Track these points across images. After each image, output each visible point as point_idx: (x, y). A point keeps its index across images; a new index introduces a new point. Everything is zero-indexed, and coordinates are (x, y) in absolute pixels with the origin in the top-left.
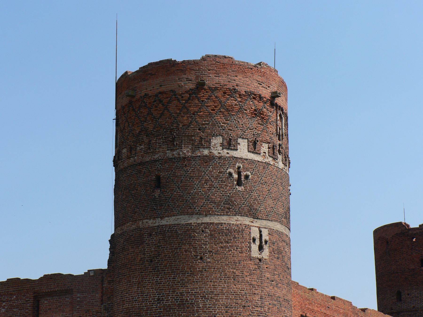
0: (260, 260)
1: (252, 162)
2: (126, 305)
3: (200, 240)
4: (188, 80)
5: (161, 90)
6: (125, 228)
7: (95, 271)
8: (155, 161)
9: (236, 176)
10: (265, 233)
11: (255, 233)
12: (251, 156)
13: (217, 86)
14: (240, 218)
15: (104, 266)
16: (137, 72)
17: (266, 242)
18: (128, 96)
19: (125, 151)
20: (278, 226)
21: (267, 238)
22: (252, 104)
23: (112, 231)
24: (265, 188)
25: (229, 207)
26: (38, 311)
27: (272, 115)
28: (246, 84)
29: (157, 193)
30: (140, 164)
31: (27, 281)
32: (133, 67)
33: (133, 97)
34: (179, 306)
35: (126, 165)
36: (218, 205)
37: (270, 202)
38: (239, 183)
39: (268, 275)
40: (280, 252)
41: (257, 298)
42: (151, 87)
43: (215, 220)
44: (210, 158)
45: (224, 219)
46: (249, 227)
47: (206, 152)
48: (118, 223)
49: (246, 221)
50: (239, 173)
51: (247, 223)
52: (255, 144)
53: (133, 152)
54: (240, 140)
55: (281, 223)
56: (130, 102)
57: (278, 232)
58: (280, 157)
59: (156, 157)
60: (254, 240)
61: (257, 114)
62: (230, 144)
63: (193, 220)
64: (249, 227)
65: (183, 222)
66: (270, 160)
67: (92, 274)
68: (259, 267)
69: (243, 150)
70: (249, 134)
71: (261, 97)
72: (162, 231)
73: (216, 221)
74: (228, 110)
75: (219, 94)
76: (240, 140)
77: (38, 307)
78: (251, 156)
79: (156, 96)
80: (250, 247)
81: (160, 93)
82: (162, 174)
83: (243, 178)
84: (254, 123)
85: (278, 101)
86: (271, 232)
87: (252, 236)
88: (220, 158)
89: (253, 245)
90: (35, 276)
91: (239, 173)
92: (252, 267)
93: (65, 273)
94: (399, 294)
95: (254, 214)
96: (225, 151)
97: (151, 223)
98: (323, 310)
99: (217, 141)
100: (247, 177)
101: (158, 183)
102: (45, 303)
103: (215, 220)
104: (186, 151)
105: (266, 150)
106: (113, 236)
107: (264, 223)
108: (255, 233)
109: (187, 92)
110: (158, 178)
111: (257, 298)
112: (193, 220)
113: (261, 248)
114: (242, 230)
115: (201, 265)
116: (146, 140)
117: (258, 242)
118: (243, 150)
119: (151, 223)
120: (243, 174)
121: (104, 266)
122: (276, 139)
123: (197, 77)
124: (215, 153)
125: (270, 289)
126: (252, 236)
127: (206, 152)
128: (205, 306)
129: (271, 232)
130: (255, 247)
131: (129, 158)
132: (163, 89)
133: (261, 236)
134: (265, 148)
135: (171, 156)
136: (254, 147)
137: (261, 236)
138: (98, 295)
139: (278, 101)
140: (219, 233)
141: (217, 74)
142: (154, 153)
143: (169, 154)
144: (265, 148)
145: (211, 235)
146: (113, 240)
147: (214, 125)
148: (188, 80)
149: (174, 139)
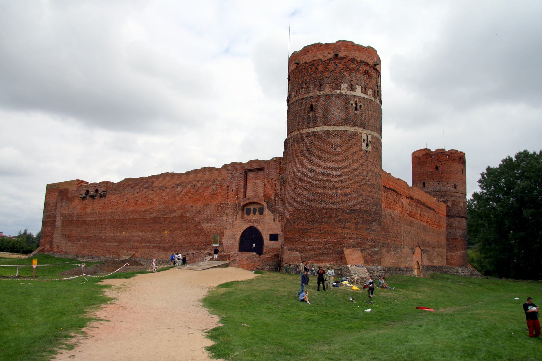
0: (367, 152)
1: (363, 98)
2: (293, 174)
3: (334, 139)
4: (328, 53)
5: (314, 59)
6: (293, 134)
7: (276, 158)
8: (310, 97)
9: (354, 105)
10: (370, 137)
11: (364, 137)
12: (363, 95)
13: (345, 56)
14: (356, 128)
15: (282, 156)
16: (301, 51)
17: (370, 142)
18: (296, 63)
19: (293, 93)
20: (376, 134)
21: (371, 140)
22: (363, 68)
23: (285, 137)
26: (246, 179)
27: (375, 75)
29: (311, 114)
30: (301, 99)
31: (241, 164)
32: (299, 49)
33: (298, 64)
34: (322, 175)
35: (294, 100)
36: (345, 120)
37: (373, 121)
38: (356, 109)
39: (371, 160)
40: (377, 149)
41: (365, 172)
42: (308, 58)
46: (361, 133)
47: (338, 92)
48: (289, 133)
49: (360, 130)
50: (356, 104)
51: (360, 131)
52: (365, 88)
53: (298, 93)
54: (357, 86)
55: (378, 133)
56: (297, 67)
58: (378, 98)
59: (311, 95)
60: (364, 140)
61: (366, 73)
62: (352, 88)
64: (361, 133)
65: (325, 129)
67: (274, 160)
68: (366, 155)
69: (358, 92)
70: (362, 83)
71: (368, 64)
72: (313, 135)
73: (343, 129)
74: (350, 70)
75: (346, 61)
76: (357, 86)
77: (246, 177)
78: (363, 95)
79: (311, 62)
80: (362, 144)
81: (314, 61)
82: (314, 104)
83: (358, 107)
84: (365, 77)
85: (377, 67)
87: (363, 138)
88: (346, 95)
89: (363, 143)
91: (356, 104)
92: (363, 155)
93: (260, 159)
94: (424, 184)
95: (364, 126)
96: (349, 91)
97: (307, 130)
98: (394, 184)
99: (344, 86)
100: (361, 106)
101: (312, 108)
102: (250, 175)
105: (371, 93)
107: (369, 132)
108: (364, 137)
109: (328, 60)
110: (312, 106)
111: (365, 172)
113: (367, 145)
114: (357, 135)
116: (305, 86)
117: (366, 142)
118: (358, 92)
119: (307, 130)
120: (359, 104)
121: (282, 156)
122: (376, 87)
123: (334, 52)
124: (344, 92)
126: (363, 138)
127: (338, 92)
128: (336, 175)
130: (364, 144)
131: (296, 97)
132: (315, 59)
133: (367, 138)
134: (370, 91)
135: (319, 94)
136: (364, 90)
137: (367, 138)
138: (278, 171)
139: (377, 67)
142: (310, 93)
143: (318, 93)
144: (370, 91)
145: (340, 137)
146: (286, 142)
147: (342, 77)
148: (328, 53)
149: (321, 85)
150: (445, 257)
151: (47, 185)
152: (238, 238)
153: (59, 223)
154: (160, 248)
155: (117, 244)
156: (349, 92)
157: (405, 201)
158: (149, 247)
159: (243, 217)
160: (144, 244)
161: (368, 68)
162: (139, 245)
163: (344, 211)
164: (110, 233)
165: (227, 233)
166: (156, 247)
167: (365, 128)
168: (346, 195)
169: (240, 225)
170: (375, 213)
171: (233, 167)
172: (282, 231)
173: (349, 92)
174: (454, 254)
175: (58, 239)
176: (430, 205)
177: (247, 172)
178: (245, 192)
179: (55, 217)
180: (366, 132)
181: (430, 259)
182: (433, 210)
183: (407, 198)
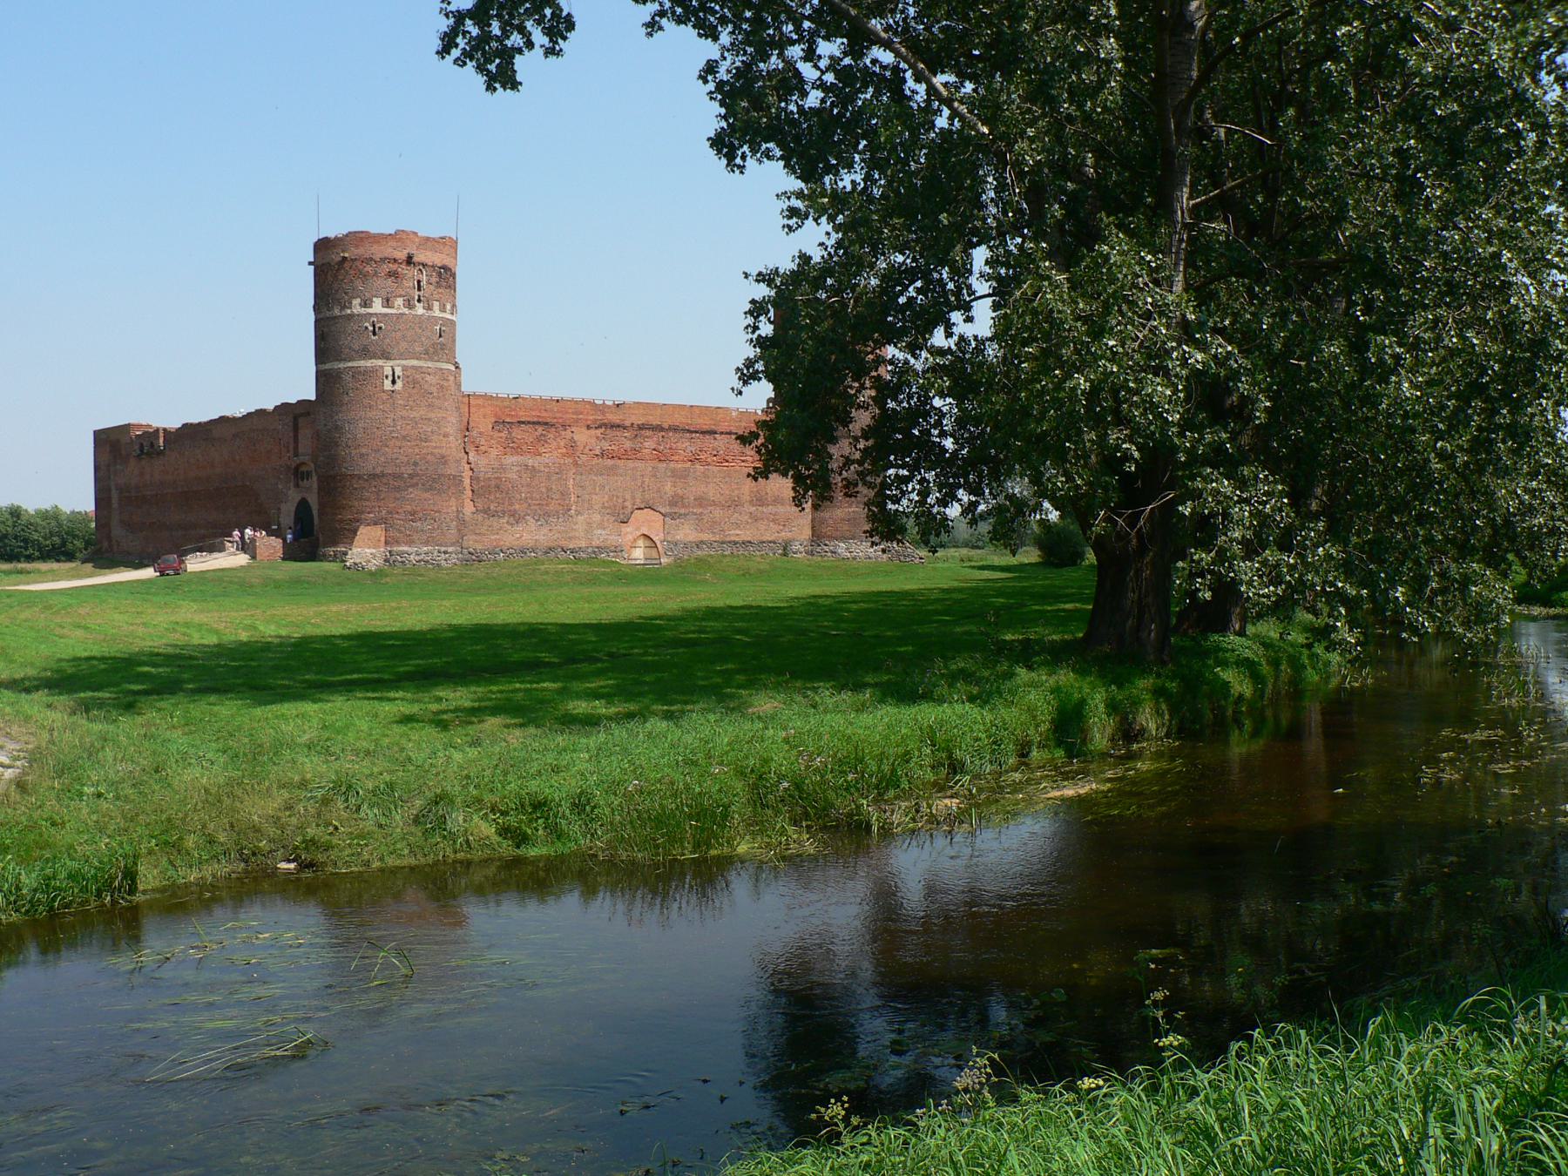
1: (386, 315)
22: (387, 267)
24: (399, 334)
25: (366, 353)
28: (378, 251)
43: (355, 364)
44: (352, 316)
45: (362, 363)
49: (380, 362)
57: (413, 367)
61: (393, 274)
62: (366, 304)
63: (341, 365)
66: (406, 311)
69: (377, 307)
86: (405, 368)
90: (294, 401)
95: (386, 356)
99: (356, 302)
103: (355, 364)
104: (337, 312)
108: (388, 371)
112: (341, 365)
113: (394, 382)
114: (375, 371)
115: (347, 399)
121: (313, 398)
125: (404, 413)
129: (405, 368)
130: (388, 384)
136: (387, 302)
140: (356, 372)
141: (357, 246)
144: (400, 301)
151: (95, 432)
153: (115, 504)
156: (363, 311)
157: (582, 436)
159: (297, 485)
161: (393, 267)
165: (284, 507)
169: (294, 497)
170: (411, 476)
171: (284, 407)
173: (363, 311)
175: (117, 531)
176: (706, 428)
177: (296, 418)
178: (296, 448)
179: (110, 490)
180: (391, 363)
183: (588, 427)
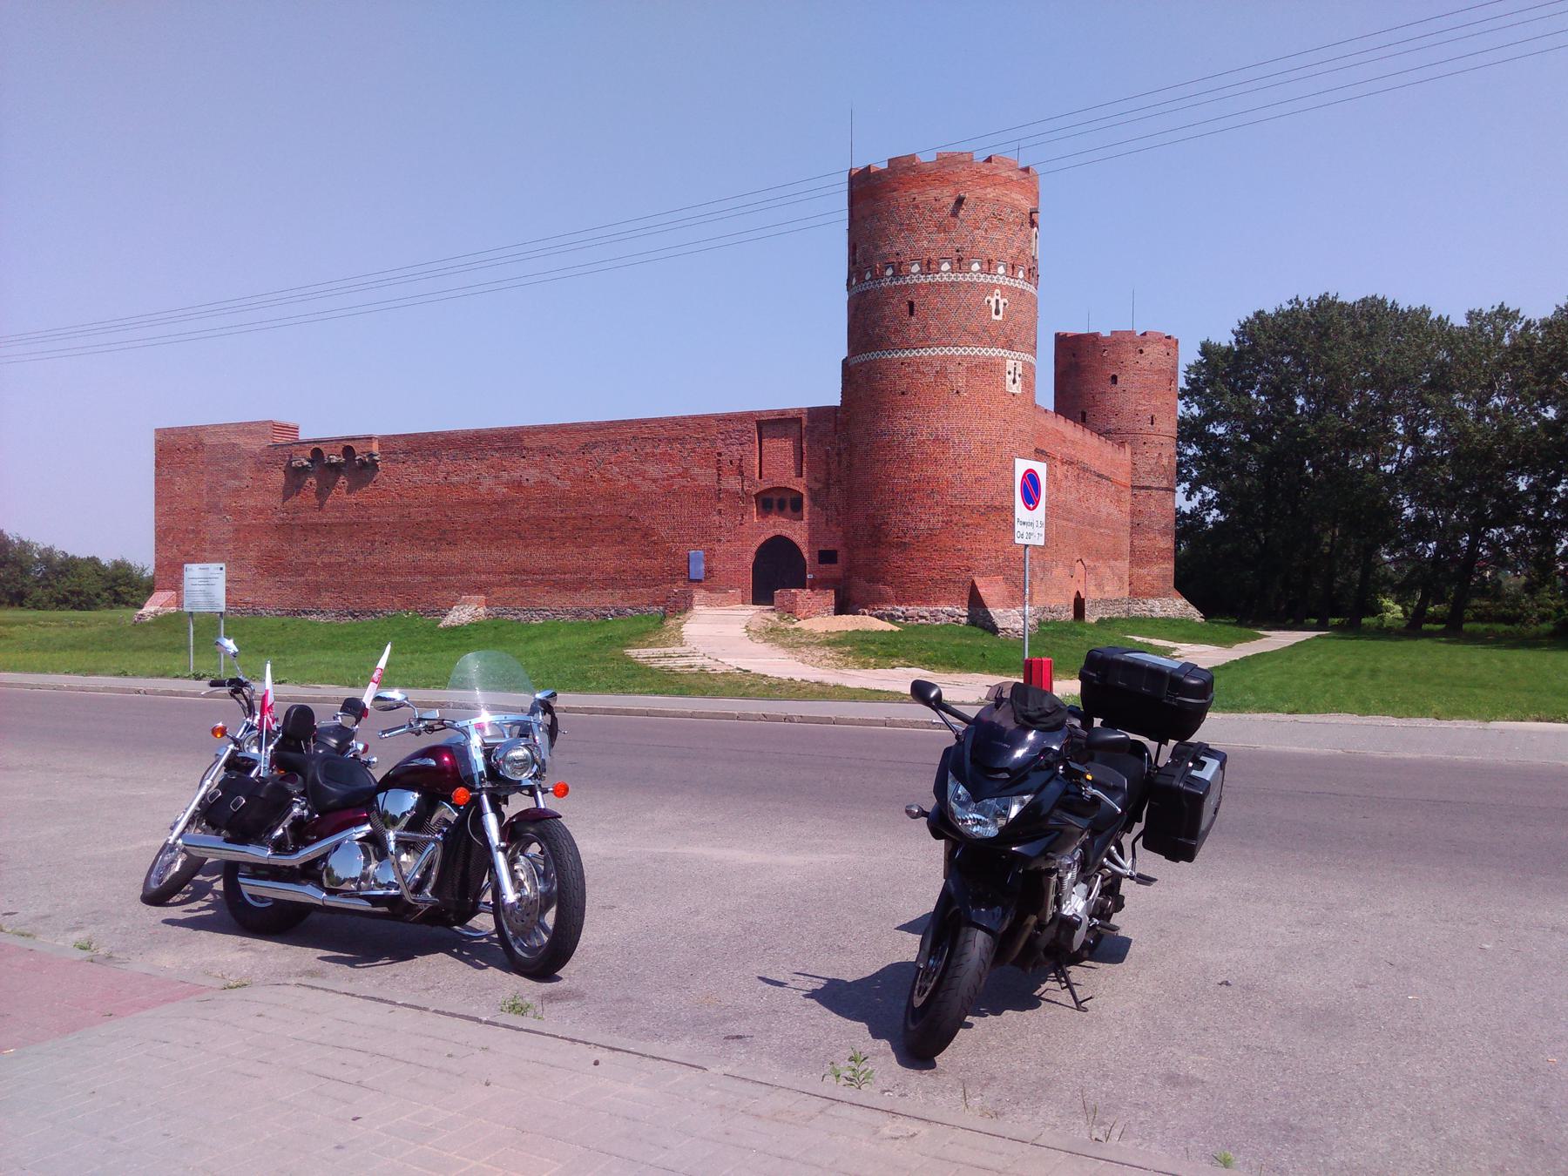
11: (1010, 365)
20: (1028, 358)
49: (1003, 352)
106: (845, 363)
130: (1009, 378)
150: (1126, 578)
152: (750, 559)
154: (555, 584)
155: (427, 579)
158: (523, 584)
160: (508, 577)
162: (492, 578)
163: (973, 509)
164: (402, 555)
166: (541, 582)
167: (1011, 348)
168: (977, 480)
172: (845, 545)
174: (1143, 571)
181: (1100, 586)
182: (1107, 479)
